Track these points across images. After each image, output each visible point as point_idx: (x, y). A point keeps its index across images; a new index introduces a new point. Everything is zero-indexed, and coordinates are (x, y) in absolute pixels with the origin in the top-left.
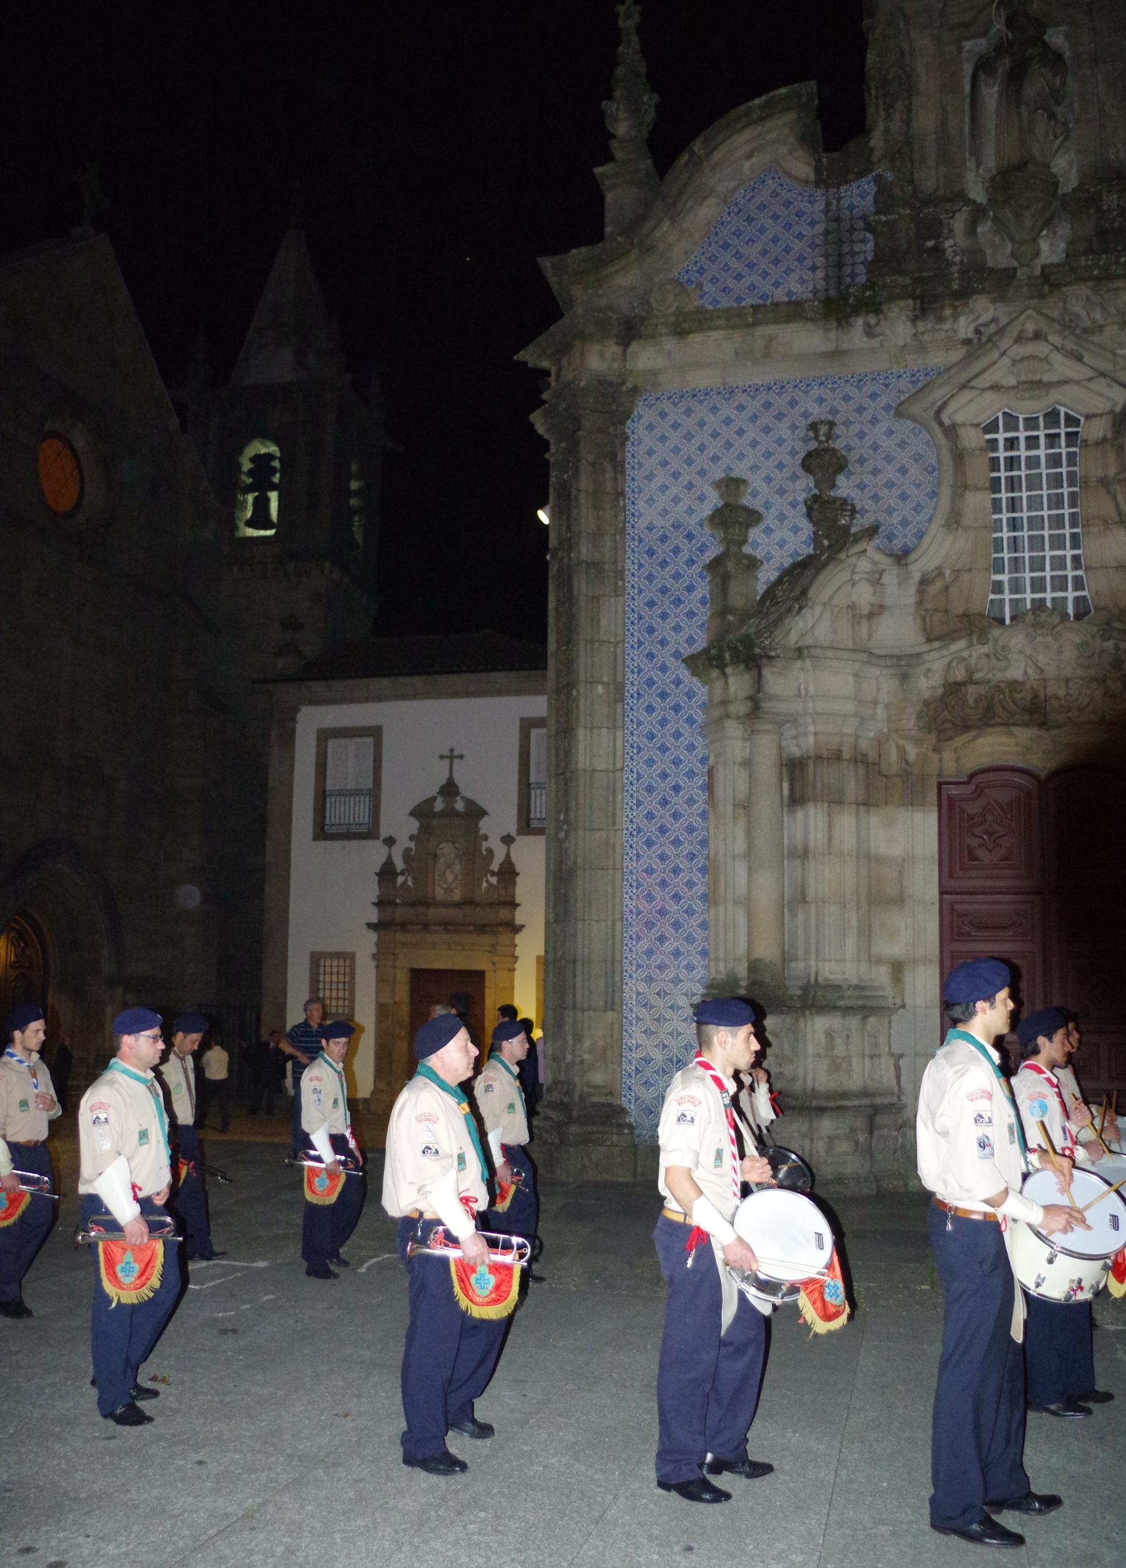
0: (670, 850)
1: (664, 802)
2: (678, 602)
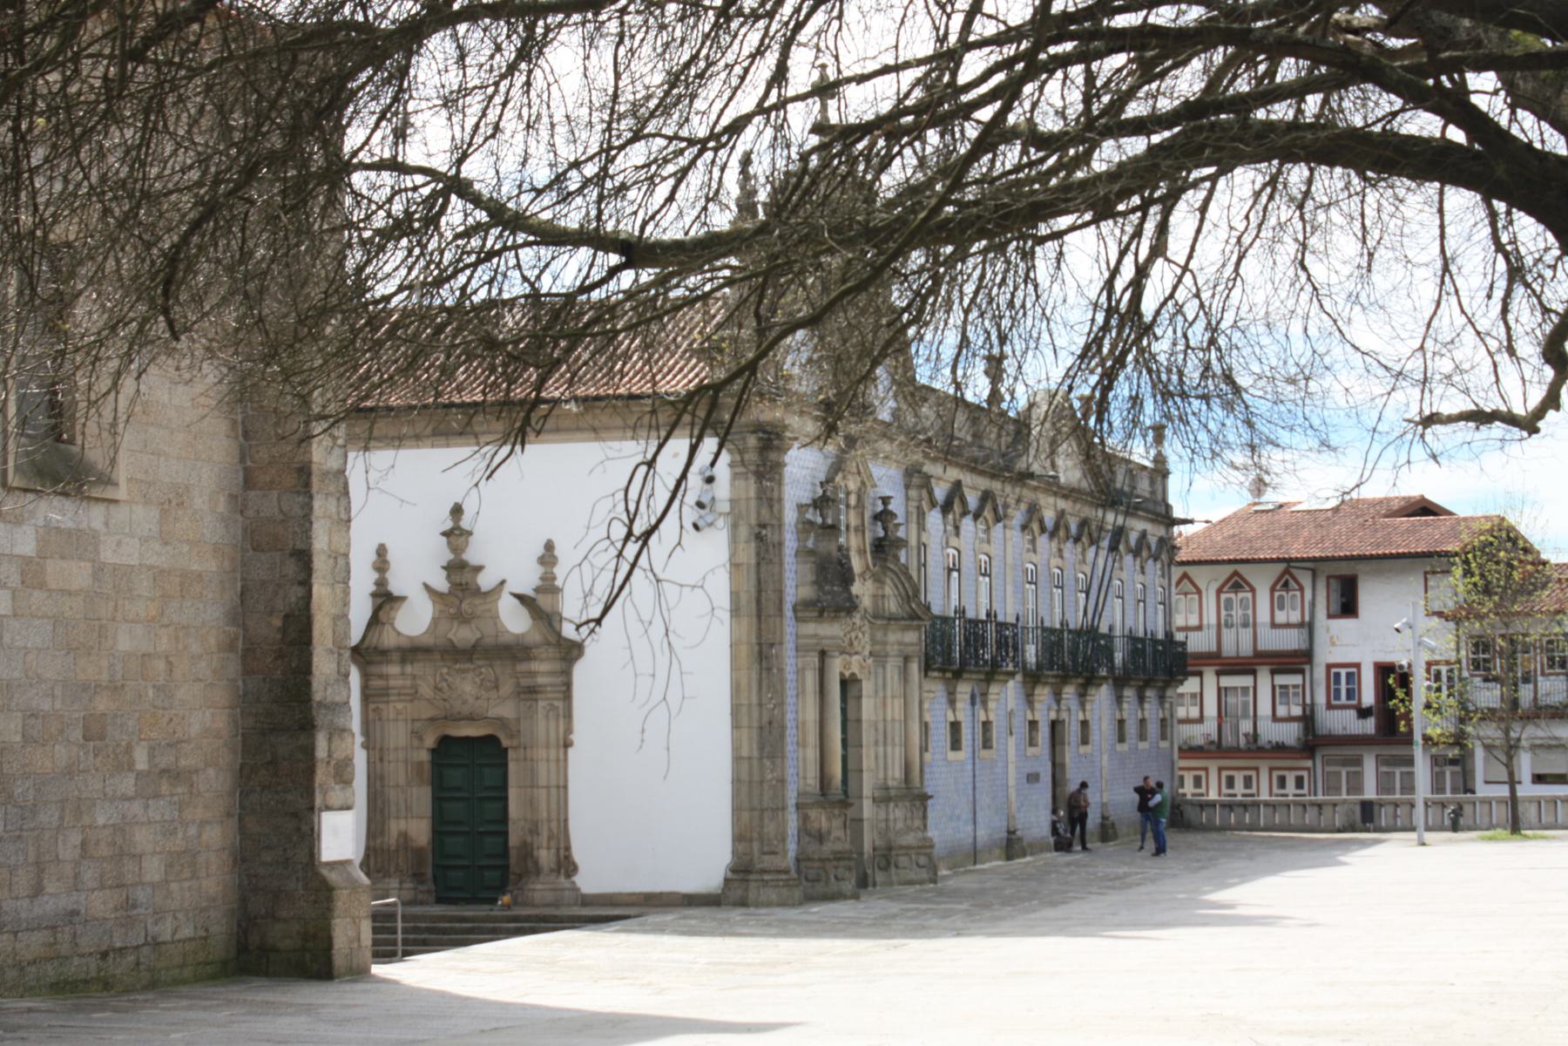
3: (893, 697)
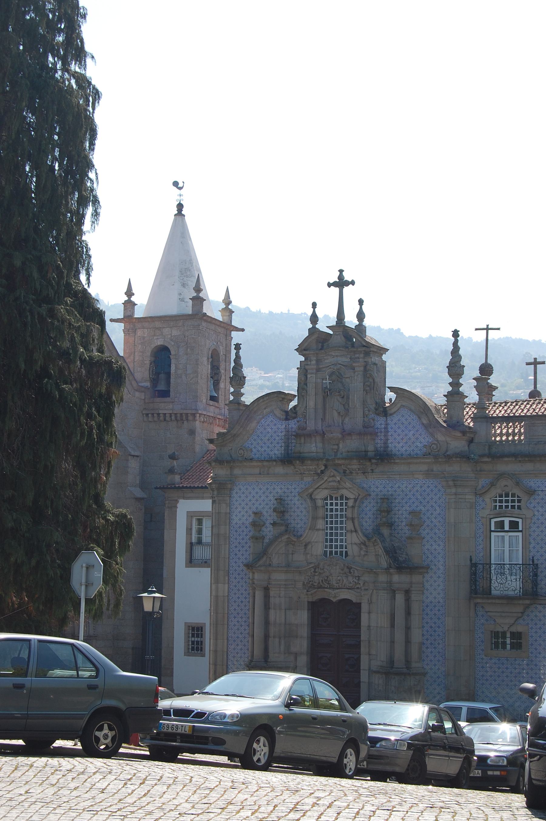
0: (240, 620)
1: (239, 606)
2: (243, 547)
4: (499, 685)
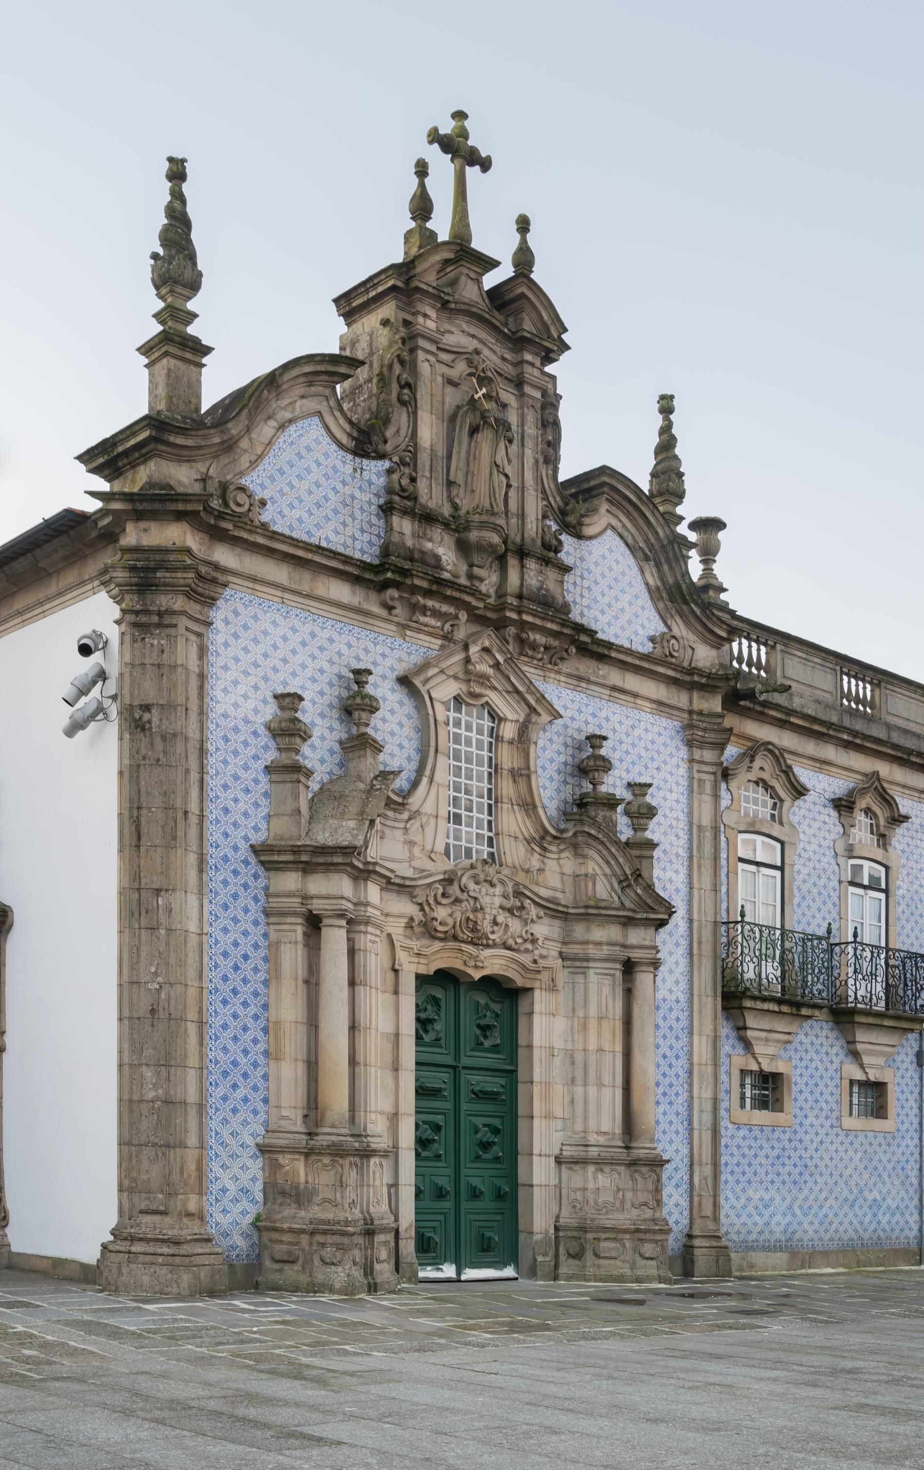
0: (240, 1011)
1: (236, 968)
3: (600, 1018)
4: (749, 1182)
